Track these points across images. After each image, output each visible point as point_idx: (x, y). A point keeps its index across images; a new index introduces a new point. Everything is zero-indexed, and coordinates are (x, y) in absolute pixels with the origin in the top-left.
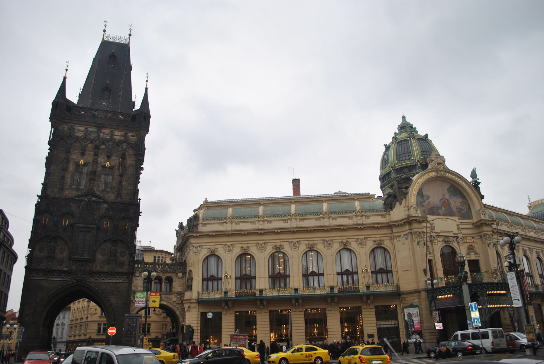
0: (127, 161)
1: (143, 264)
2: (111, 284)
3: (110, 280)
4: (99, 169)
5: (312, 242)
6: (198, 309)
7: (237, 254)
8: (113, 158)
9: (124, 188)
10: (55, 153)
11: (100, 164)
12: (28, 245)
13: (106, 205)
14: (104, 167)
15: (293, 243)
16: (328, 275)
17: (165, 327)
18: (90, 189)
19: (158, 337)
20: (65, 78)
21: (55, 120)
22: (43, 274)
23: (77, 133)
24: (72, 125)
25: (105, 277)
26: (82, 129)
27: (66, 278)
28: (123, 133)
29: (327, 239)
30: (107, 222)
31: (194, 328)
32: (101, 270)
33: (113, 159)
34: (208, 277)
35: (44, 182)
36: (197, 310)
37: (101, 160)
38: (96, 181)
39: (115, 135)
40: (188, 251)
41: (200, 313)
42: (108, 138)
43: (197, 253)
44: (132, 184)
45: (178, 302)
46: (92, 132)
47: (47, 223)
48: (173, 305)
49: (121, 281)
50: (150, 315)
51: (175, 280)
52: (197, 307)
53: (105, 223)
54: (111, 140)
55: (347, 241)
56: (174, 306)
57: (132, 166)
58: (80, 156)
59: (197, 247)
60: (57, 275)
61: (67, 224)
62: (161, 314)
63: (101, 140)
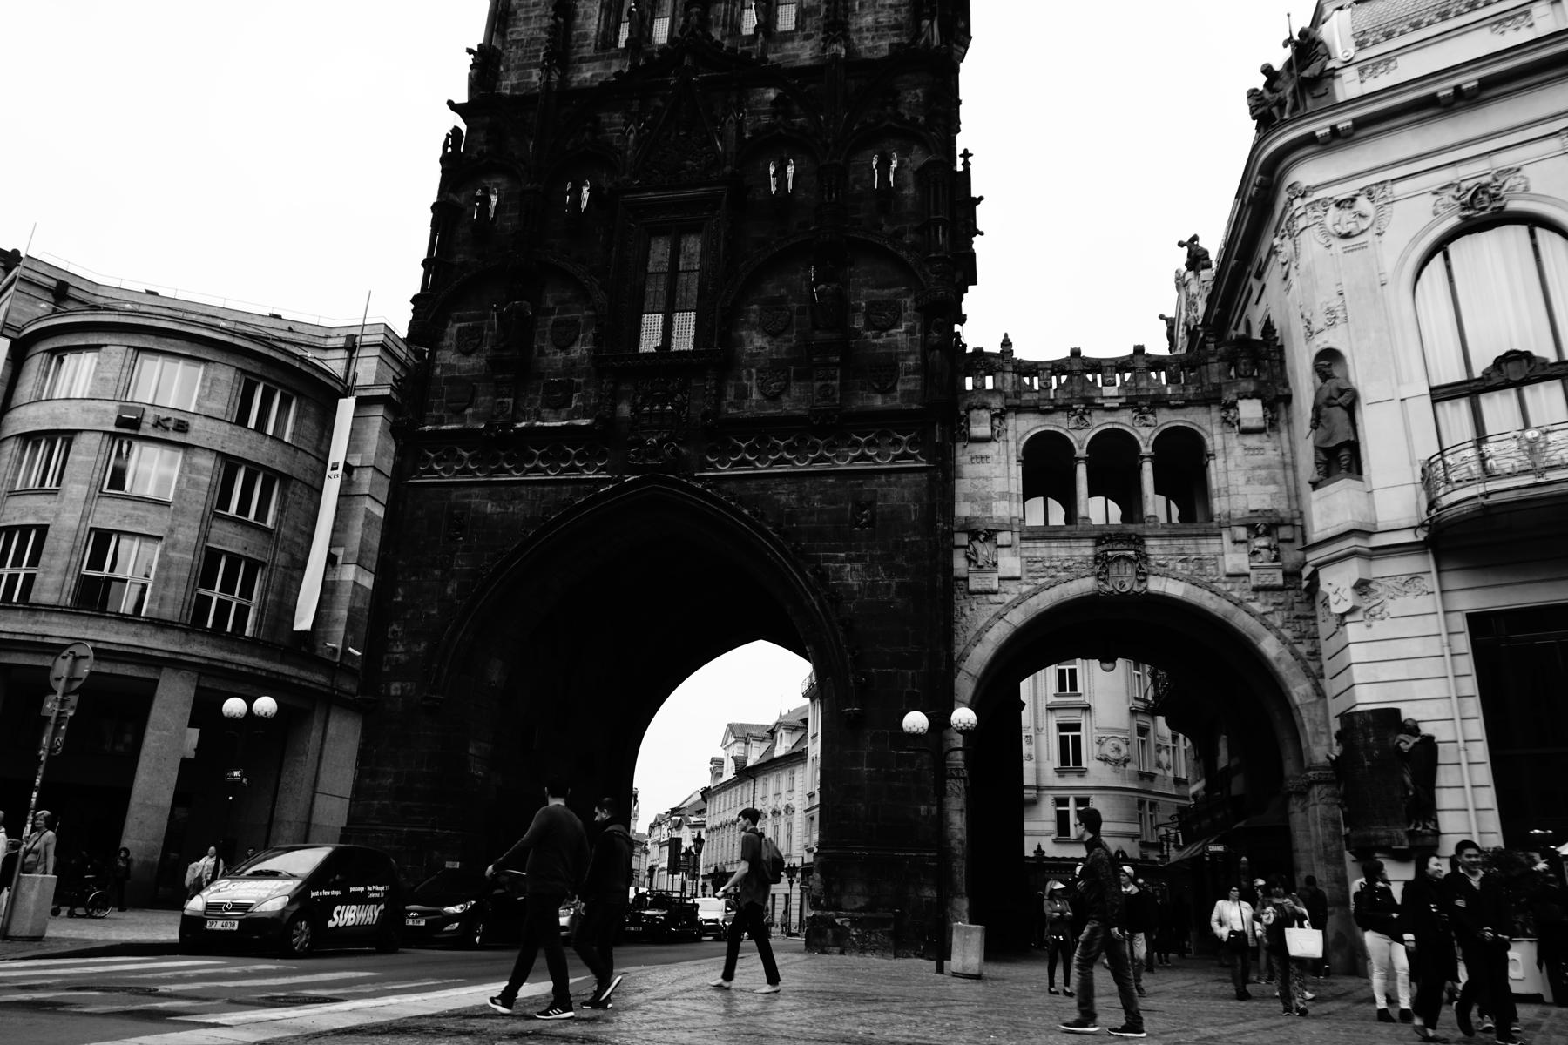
1: (1010, 368)
3: (822, 459)
17: (1149, 813)
18: (690, 29)
19: (1123, 852)
22: (473, 459)
25: (789, 448)
27: (586, 467)
31: (1426, 729)
34: (1477, 374)
35: (480, 46)
36: (1431, 603)
40: (1286, 247)
41: (1460, 623)
43: (1362, 232)
45: (1266, 580)
47: (492, 214)
48: (1225, 596)
49: (885, 464)
50: (1084, 765)
51: (1219, 447)
52: (1431, 582)
53: (772, 170)
56: (1239, 604)
59: (1353, 200)
60: (543, 458)
61: (584, 205)
62: (1127, 761)
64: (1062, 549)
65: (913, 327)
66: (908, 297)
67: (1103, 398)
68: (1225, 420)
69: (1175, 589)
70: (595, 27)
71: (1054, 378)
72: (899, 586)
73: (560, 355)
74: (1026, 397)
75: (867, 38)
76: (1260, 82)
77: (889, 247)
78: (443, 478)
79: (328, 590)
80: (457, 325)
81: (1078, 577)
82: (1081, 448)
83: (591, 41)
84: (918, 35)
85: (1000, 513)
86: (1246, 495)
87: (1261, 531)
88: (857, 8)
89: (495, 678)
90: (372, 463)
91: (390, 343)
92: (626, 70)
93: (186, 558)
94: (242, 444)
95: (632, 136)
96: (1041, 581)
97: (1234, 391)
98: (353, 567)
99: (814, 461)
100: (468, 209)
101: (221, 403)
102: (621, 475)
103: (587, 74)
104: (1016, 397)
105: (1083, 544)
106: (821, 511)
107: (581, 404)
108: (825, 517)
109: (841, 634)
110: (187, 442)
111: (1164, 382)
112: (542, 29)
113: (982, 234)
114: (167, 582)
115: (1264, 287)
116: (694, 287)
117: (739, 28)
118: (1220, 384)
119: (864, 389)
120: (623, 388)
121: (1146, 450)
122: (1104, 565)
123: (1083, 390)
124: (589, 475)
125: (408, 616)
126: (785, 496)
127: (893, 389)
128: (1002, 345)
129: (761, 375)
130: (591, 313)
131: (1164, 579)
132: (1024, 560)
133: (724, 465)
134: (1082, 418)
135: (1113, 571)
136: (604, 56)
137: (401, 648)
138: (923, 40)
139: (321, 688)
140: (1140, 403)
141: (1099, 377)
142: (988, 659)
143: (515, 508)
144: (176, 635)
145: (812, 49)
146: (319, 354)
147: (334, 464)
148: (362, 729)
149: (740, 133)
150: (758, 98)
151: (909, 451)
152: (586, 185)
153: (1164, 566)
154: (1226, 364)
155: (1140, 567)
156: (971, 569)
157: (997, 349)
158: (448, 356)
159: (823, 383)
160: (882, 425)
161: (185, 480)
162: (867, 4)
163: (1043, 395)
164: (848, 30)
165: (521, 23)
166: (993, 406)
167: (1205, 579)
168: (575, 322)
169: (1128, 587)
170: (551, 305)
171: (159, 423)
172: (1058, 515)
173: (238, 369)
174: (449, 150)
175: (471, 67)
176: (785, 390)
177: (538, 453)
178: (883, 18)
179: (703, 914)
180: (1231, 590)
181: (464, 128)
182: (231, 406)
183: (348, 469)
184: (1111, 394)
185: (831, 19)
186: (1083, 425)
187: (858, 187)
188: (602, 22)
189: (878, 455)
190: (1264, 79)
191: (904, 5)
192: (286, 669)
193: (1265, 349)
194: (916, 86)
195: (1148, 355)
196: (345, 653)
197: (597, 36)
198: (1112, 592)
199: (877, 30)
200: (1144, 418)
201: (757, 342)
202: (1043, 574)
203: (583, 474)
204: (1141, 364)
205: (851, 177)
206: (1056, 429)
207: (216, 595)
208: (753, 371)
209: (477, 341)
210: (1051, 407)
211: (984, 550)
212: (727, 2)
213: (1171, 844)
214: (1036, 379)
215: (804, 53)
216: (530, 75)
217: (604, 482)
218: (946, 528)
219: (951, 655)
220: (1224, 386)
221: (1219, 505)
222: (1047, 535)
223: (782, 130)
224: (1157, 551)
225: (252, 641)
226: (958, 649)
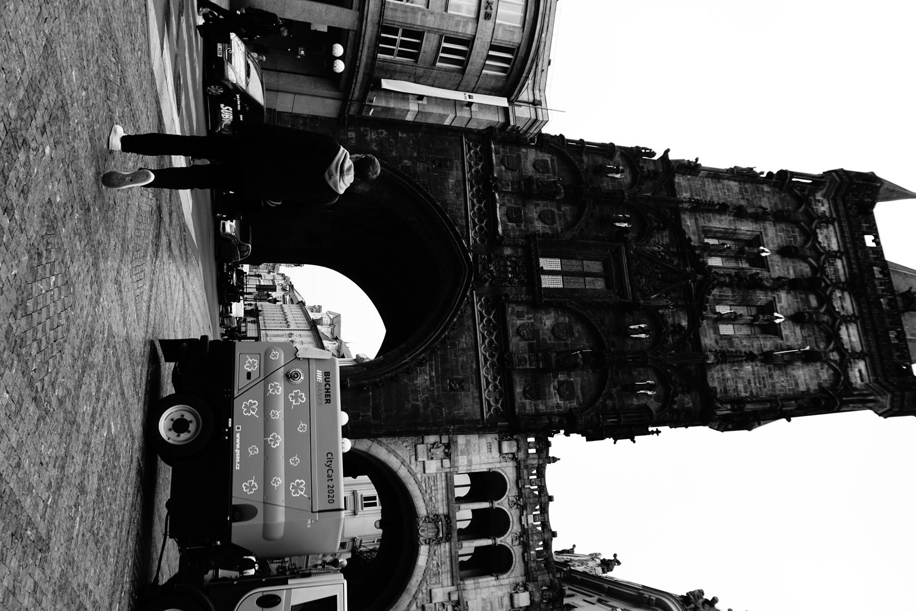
0: (801, 369)
1: (541, 462)
2: (474, 366)
3: (486, 360)
4: (762, 298)
8: (798, 330)
9: (736, 370)
10: (766, 188)
11: (774, 298)
12: (548, 133)
14: (770, 308)
18: (717, 277)
21: (837, 178)
22: (477, 171)
23: (821, 234)
25: (491, 342)
26: (835, 247)
27: (476, 232)
28: (858, 348)
32: (511, 332)
33: (794, 330)
35: (700, 164)
37: (784, 300)
38: (733, 293)
39: (847, 328)
42: (837, 310)
44: (751, 392)
46: (836, 271)
47: (610, 175)
48: (419, 590)
49: (485, 395)
51: (502, 582)
53: (643, 326)
54: (835, 319)
56: (415, 597)
57: (793, 382)
58: (776, 246)
60: (480, 209)
61: (618, 224)
63: (828, 293)
64: (441, 496)
65: (560, 407)
66: (577, 403)
67: (527, 515)
68: (517, 585)
69: (422, 560)
70: (715, 226)
71: (536, 487)
72: (417, 407)
73: (536, 215)
74: (525, 472)
75: (718, 374)
76: (708, 596)
77: (604, 392)
78: (467, 155)
79: (404, 96)
80: (549, 159)
81: (427, 505)
82: (498, 504)
83: (707, 224)
84: (723, 402)
85: (460, 460)
86: (476, 599)
87: (456, 608)
88: (735, 368)
89: (359, 187)
90: (473, 117)
91: (538, 124)
92: (692, 244)
93: (418, 21)
94: (480, 49)
95: (656, 248)
96: (423, 485)
97: (534, 589)
98: (417, 109)
99: (485, 356)
100: (612, 163)
101: (502, 37)
102: (472, 251)
103: (689, 223)
104: (525, 466)
105: (445, 508)
106: (457, 361)
107: (510, 227)
108: (454, 364)
109: (390, 375)
110: (480, 20)
111: (537, 549)
112: (712, 197)
113: (615, 443)
114: (405, 12)
115: (594, 604)
116: (577, 286)
117: (718, 304)
118: (537, 581)
119: (525, 381)
120: (520, 250)
121: (499, 541)
122: (433, 520)
123: (530, 504)
124: (472, 233)
125: (391, 140)
126: (464, 341)
127: (526, 398)
128: (553, 457)
129: (530, 325)
130: (559, 231)
131: (427, 554)
132: (435, 475)
133: (480, 306)
134: (515, 504)
135: (430, 525)
136: (699, 231)
137: (373, 137)
138: (719, 405)
139: (351, 95)
140: (525, 535)
141: (538, 512)
142: (380, 457)
143: (451, 196)
144: (376, 18)
145: (710, 344)
146: (530, 86)
147: (472, 96)
148: (330, 118)
149: (662, 307)
150: (682, 316)
151: (493, 408)
152: (629, 225)
153: (435, 554)
154: (549, 584)
155: (433, 540)
156: (429, 445)
157: (551, 454)
158: (532, 155)
159: (527, 359)
160: (506, 393)
161: (459, 19)
162: (737, 374)
163: (527, 481)
164: (722, 364)
165: (714, 186)
166: (519, 454)
167: (428, 577)
168: (554, 222)
169: (422, 534)
170: (562, 209)
172: (462, 492)
173: (520, 44)
174: (643, 151)
175: (688, 161)
176: (523, 338)
177: (482, 205)
178: (730, 383)
179: (234, 305)
180: (422, 593)
181: (656, 158)
182: (500, 42)
183: (470, 104)
184: (529, 520)
185: (728, 354)
186: (512, 504)
187: (636, 373)
188: (717, 229)
189: (489, 391)
190: (710, 599)
191: (738, 394)
192: (360, 76)
193: (558, 606)
194: (694, 403)
195: (552, 540)
196: (370, 107)
197: (710, 227)
198: (419, 525)
199: (723, 380)
200: (517, 539)
201: (548, 321)
202: (427, 486)
203: (472, 231)
204: (546, 536)
205: (641, 369)
206: (508, 489)
207: (399, 38)
208: (532, 320)
209: (541, 170)
210: (520, 486)
211: (439, 452)
212: (733, 297)
213: (280, 564)
214: (535, 477)
215: (708, 340)
216: (686, 192)
217: (468, 243)
218: (451, 431)
219: (380, 436)
220: (536, 583)
221: (469, 583)
222: (449, 488)
223: (665, 330)
224: (443, 549)
225: (374, 58)
226: (384, 440)
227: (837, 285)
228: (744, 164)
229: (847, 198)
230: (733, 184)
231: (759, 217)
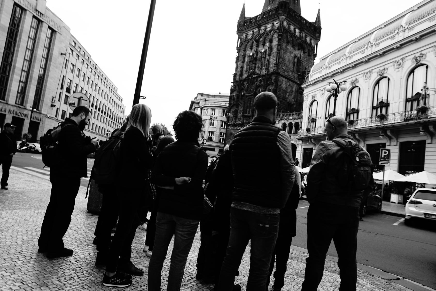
4: (259, 55)
5: (382, 68)
6: (302, 146)
7: (327, 96)
10: (240, 54)
13: (260, 79)
14: (261, 52)
15: (366, 74)
16: (394, 104)
20: (244, 4)
24: (246, 33)
29: (397, 59)
30: (260, 89)
39: (268, 28)
46: (256, 32)
55: (421, 54)
60: (238, 127)
63: (260, 35)
93: (218, 134)
121: (293, 125)
144: (216, 143)
171: (214, 118)
194: (274, 77)
207: (222, 138)
215: (264, 72)
227: (259, 32)
228: (235, 60)
229: (242, 30)
230: (238, 64)
231: (244, 56)
